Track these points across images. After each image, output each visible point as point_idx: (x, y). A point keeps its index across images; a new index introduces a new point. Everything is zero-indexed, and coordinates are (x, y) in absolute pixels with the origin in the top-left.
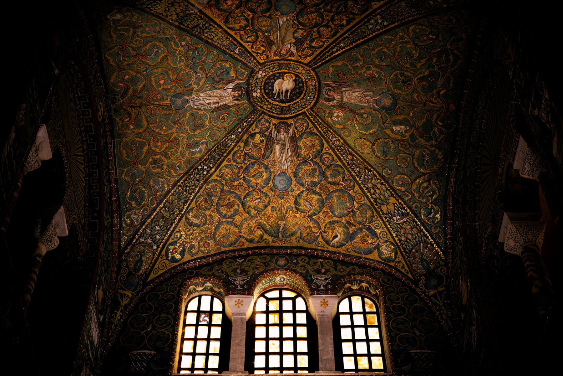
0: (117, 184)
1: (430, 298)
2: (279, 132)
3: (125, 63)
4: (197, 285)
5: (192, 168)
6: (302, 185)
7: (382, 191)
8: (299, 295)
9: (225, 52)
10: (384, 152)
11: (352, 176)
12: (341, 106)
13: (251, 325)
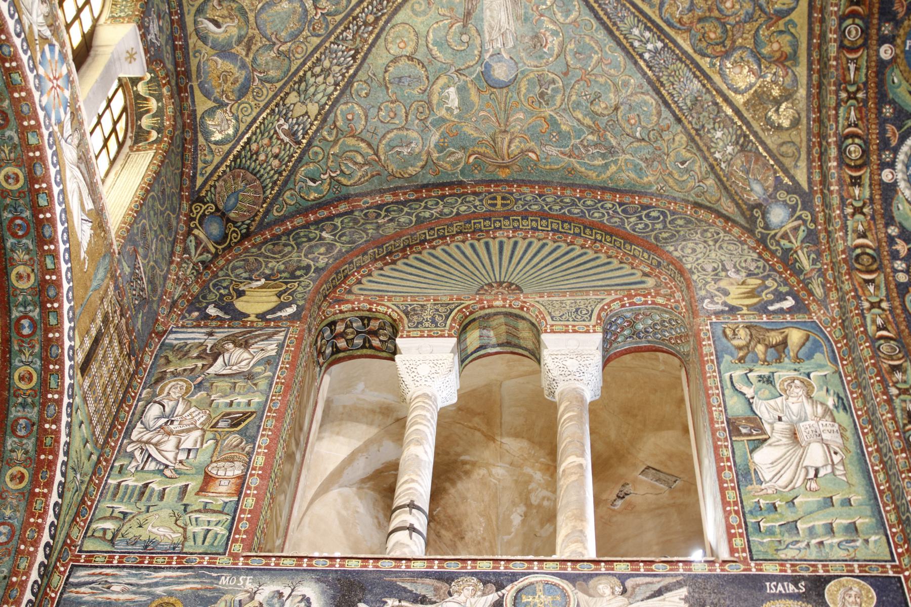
7: (322, 87)
10: (400, 78)
11: (336, 27)
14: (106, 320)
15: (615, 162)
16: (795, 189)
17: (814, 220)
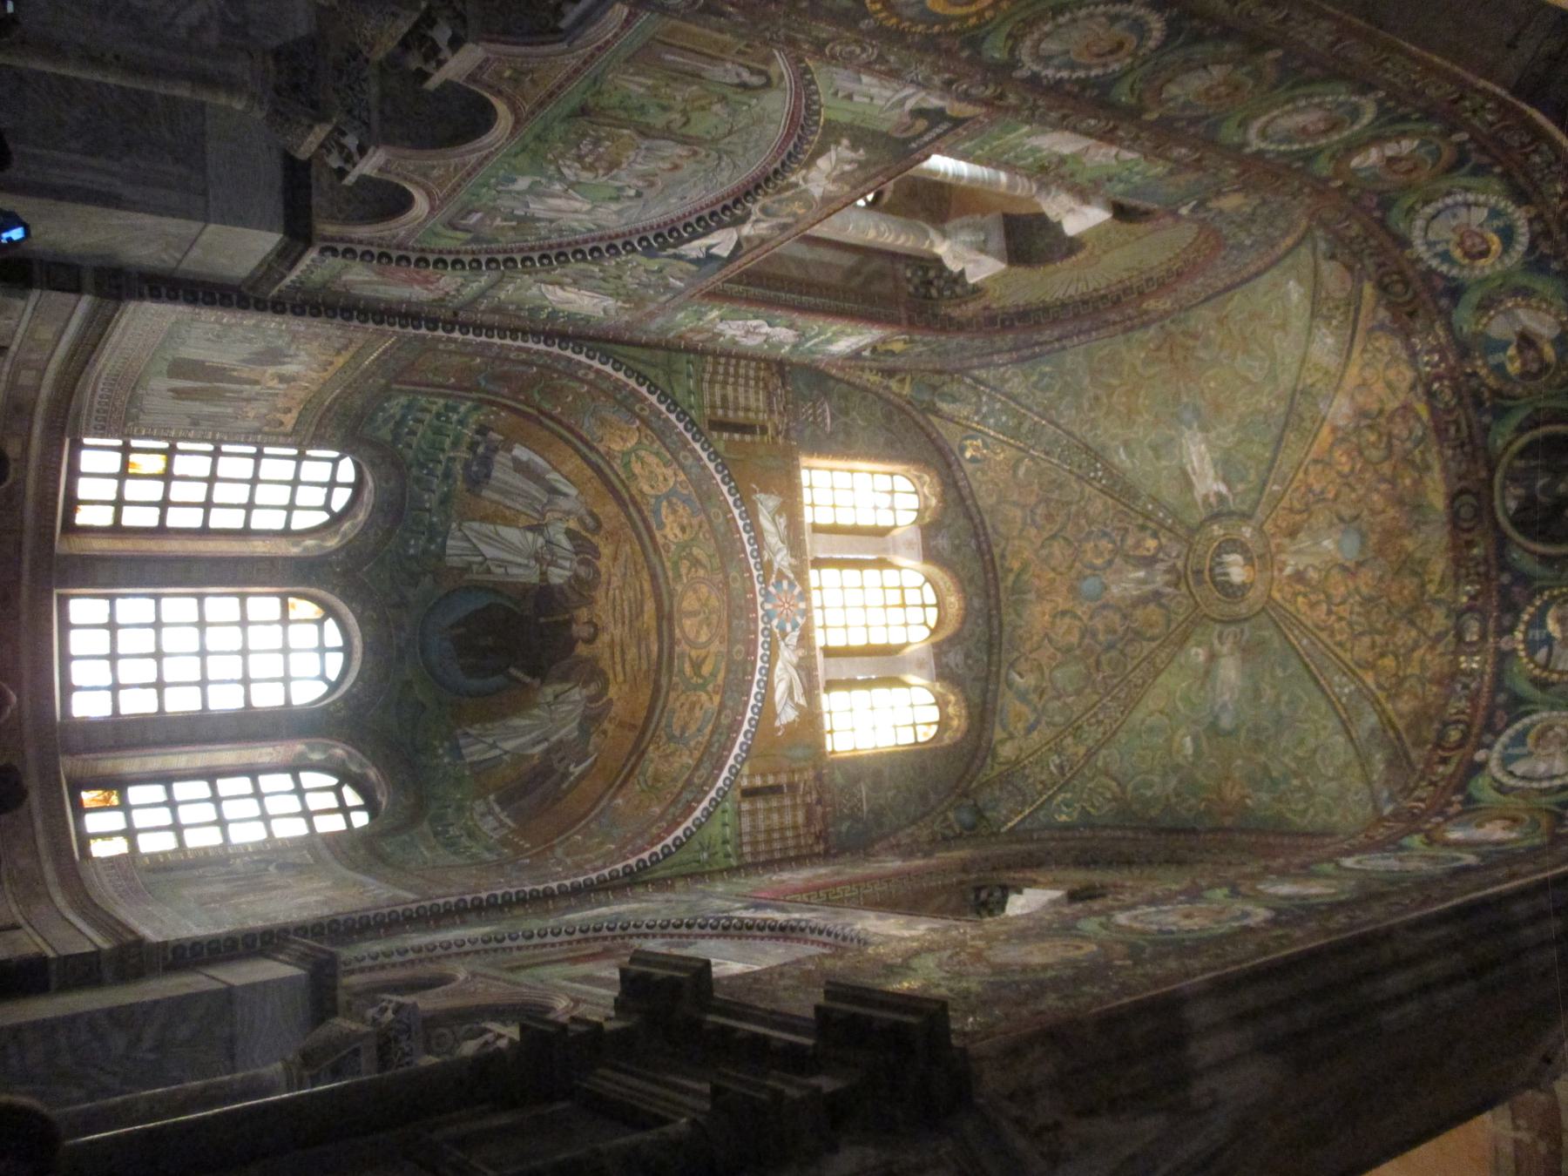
0: (1057, 351)
1: (943, 812)
2: (1167, 572)
4: (931, 486)
5: (1095, 454)
6: (1091, 618)
8: (933, 632)
9: (1270, 470)
12: (1213, 657)
13: (882, 564)
14: (793, 787)
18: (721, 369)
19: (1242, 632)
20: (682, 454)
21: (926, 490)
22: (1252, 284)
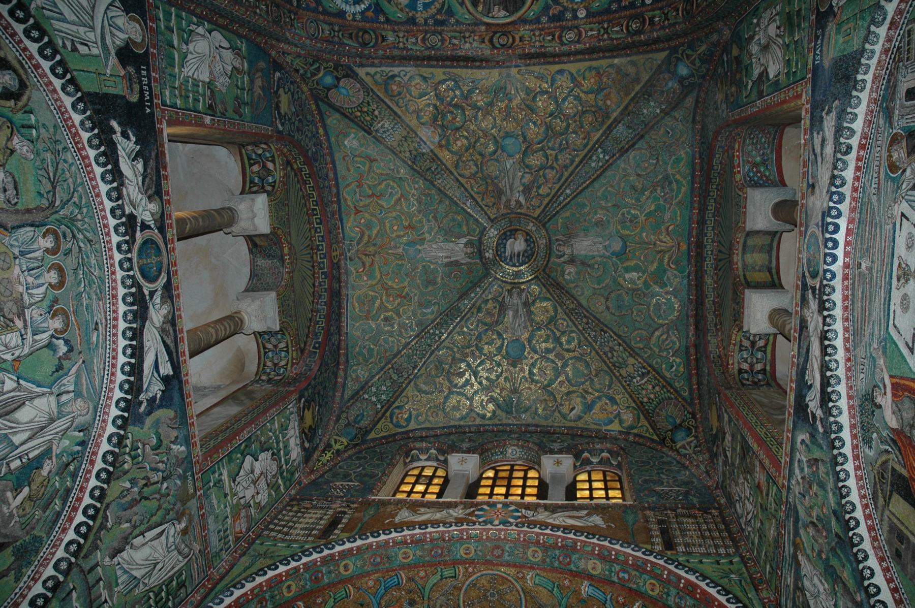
3: (361, 204)
4: (421, 450)
6: (536, 352)
8: (531, 468)
12: (572, 261)
15: (674, 175)
16: (668, 60)
17: (683, 45)
18: (278, 528)
19: (557, 240)
20: (342, 569)
21: (423, 457)
22: (340, 180)
